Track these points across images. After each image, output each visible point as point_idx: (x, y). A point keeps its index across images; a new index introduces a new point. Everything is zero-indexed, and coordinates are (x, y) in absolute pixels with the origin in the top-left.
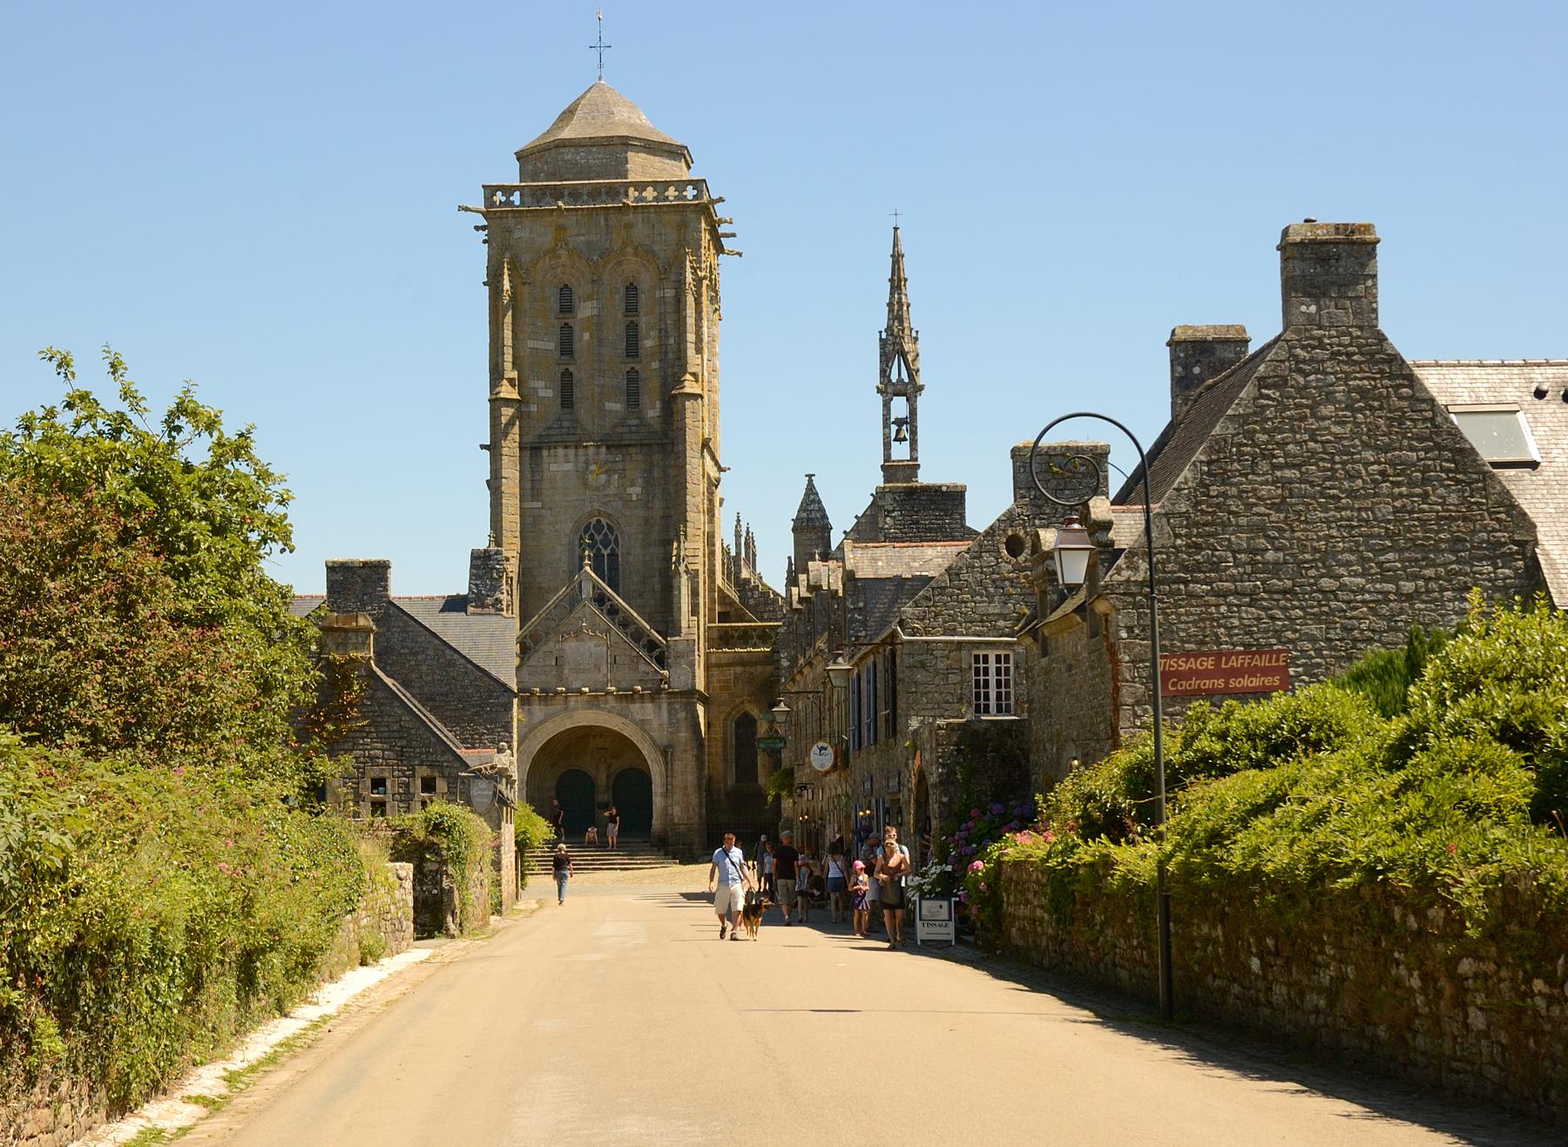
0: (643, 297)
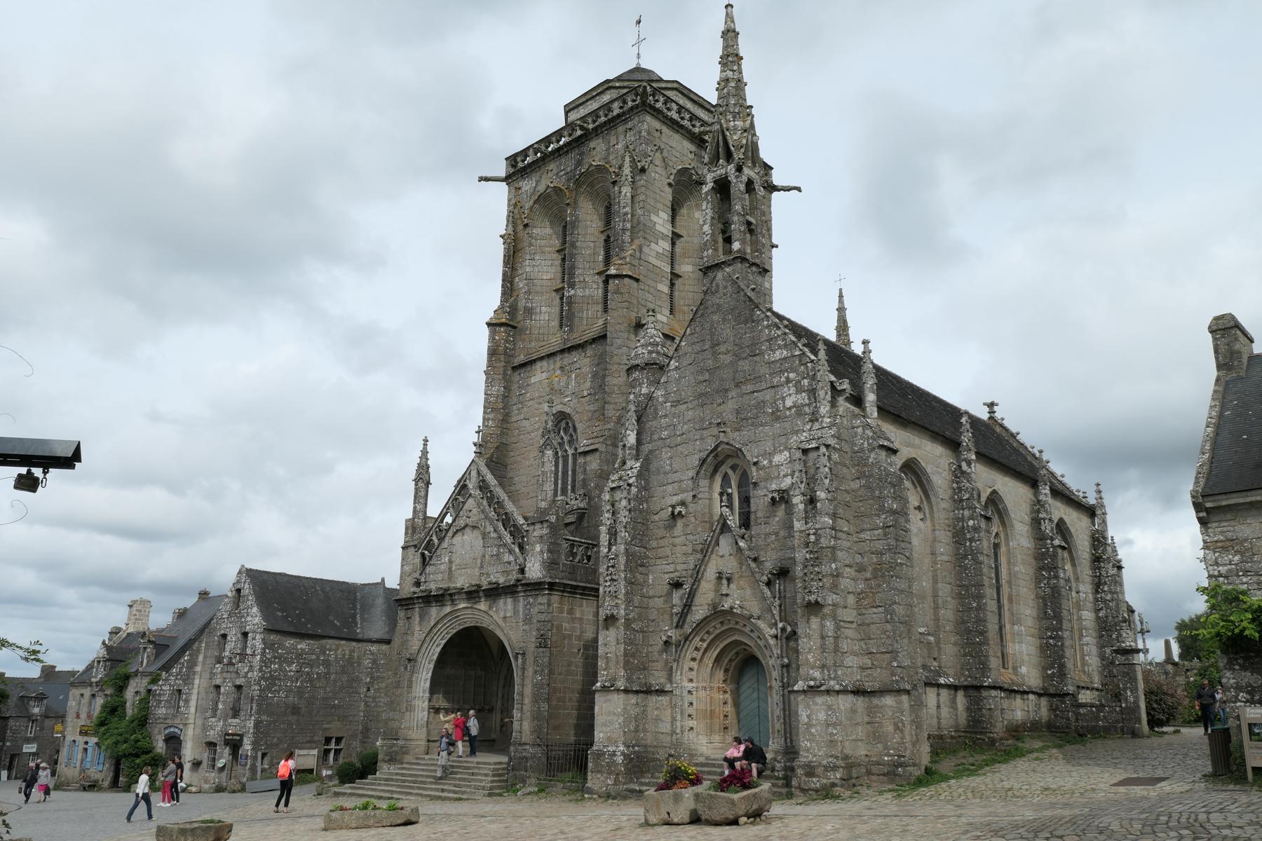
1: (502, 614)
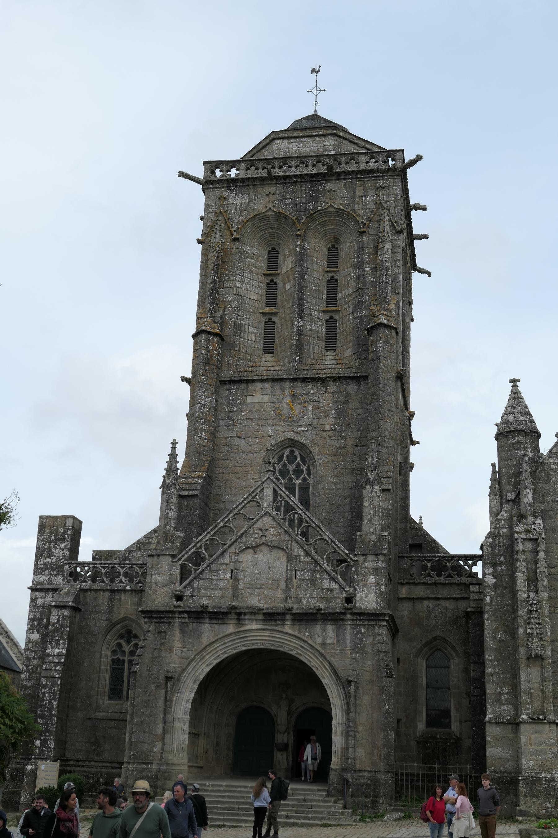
0: (342, 254)
1: (319, 640)
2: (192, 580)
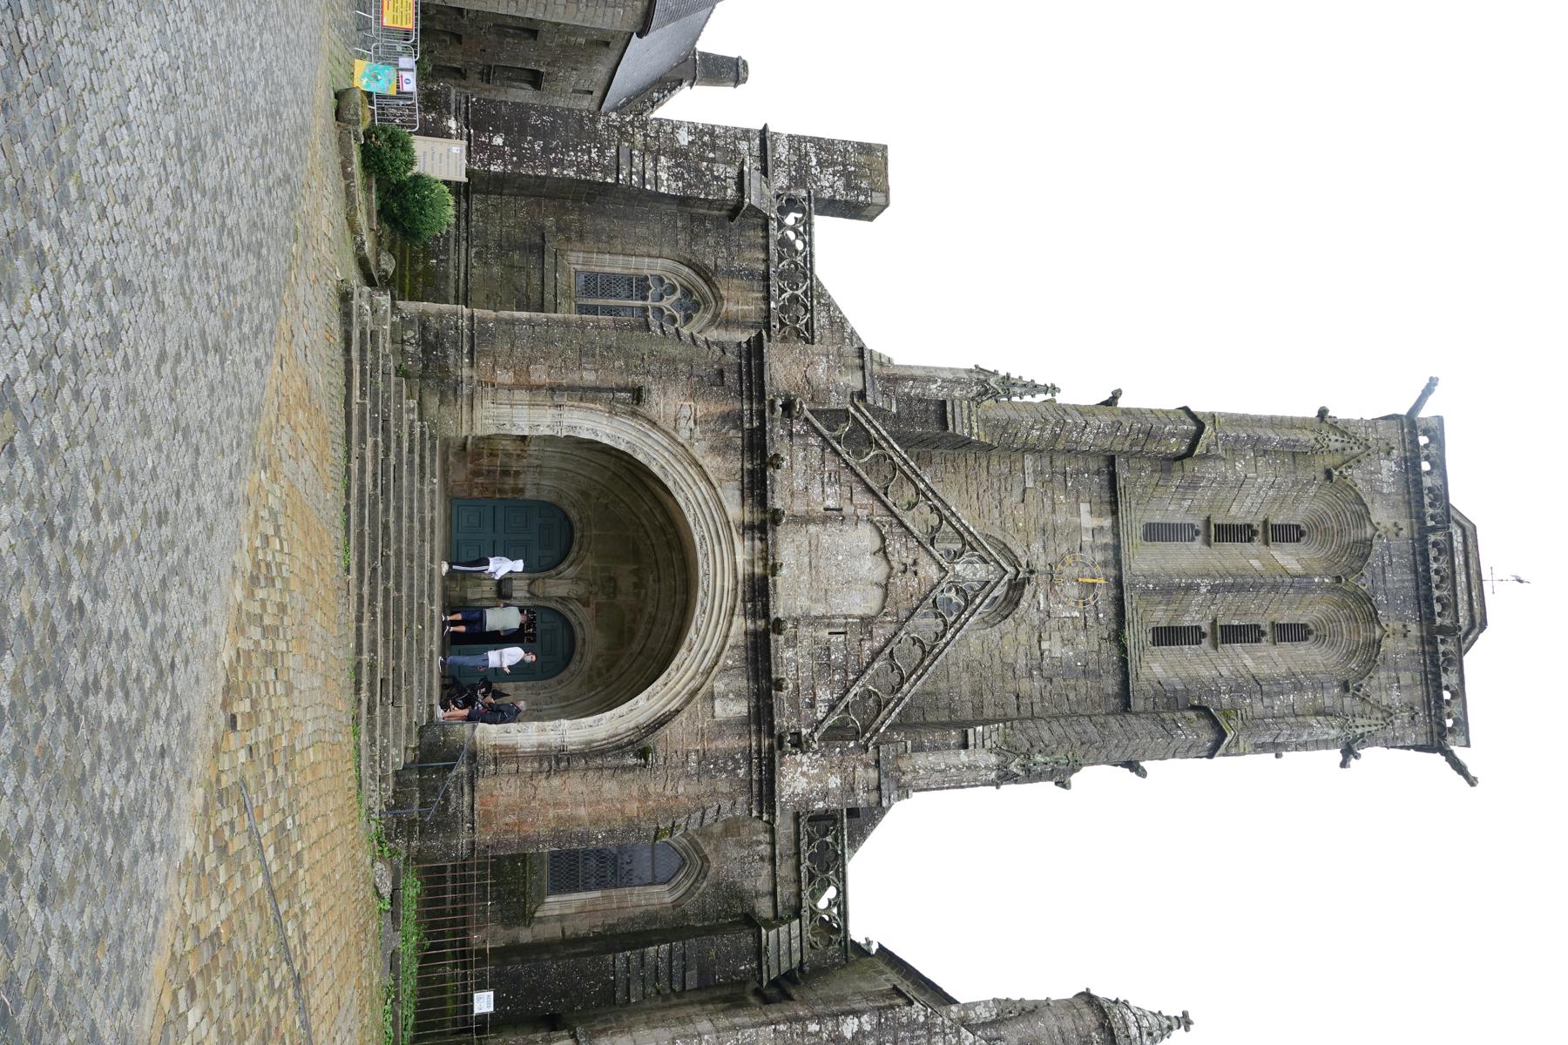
1: (719, 686)
2: (821, 435)
